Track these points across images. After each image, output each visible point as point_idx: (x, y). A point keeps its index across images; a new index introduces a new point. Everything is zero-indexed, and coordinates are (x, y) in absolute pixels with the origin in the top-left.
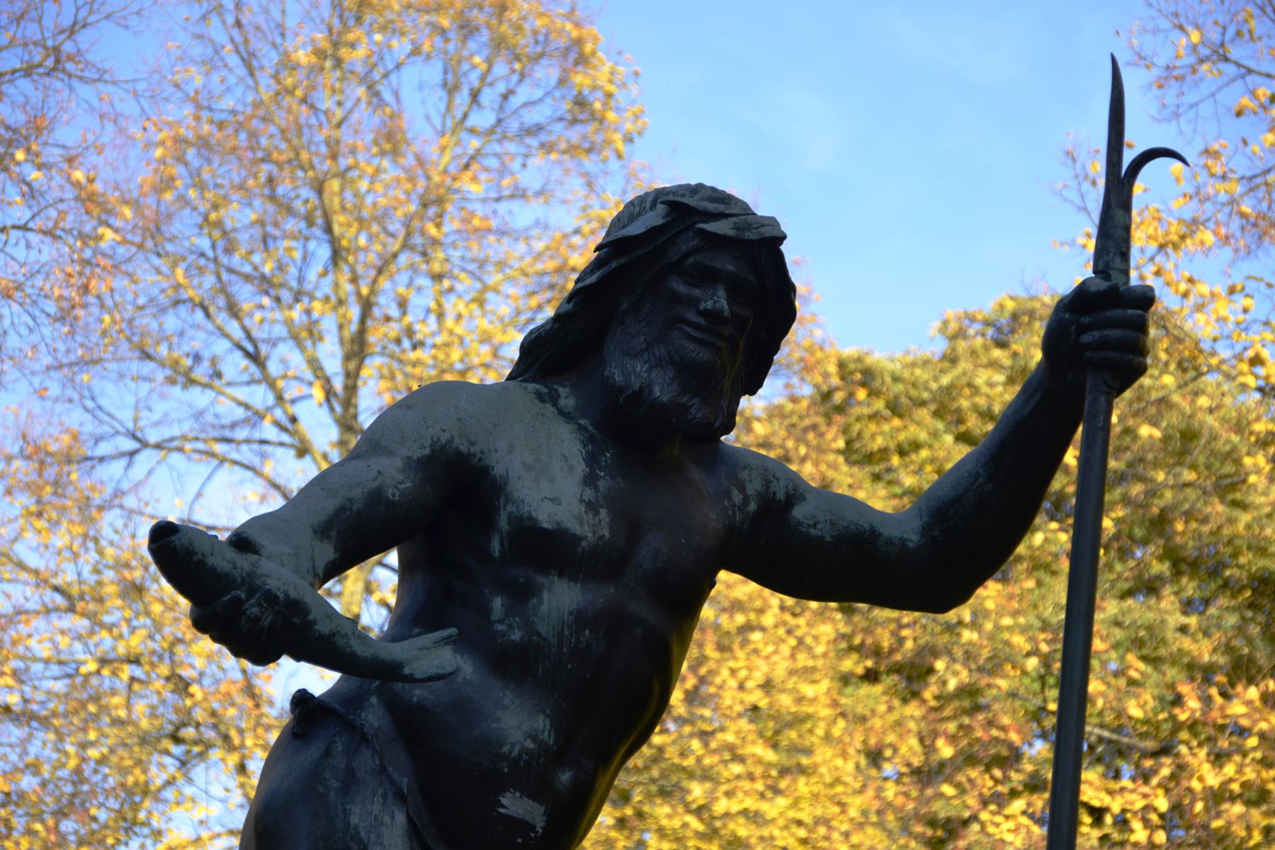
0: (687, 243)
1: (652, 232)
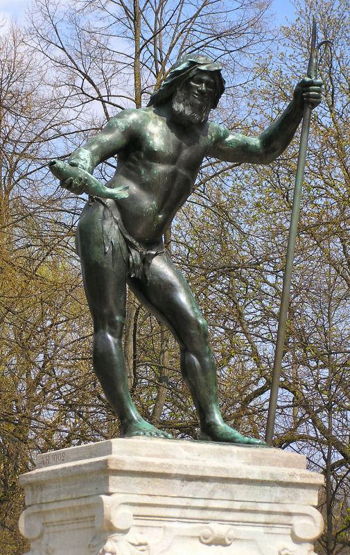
0: (194, 72)
1: (185, 69)
